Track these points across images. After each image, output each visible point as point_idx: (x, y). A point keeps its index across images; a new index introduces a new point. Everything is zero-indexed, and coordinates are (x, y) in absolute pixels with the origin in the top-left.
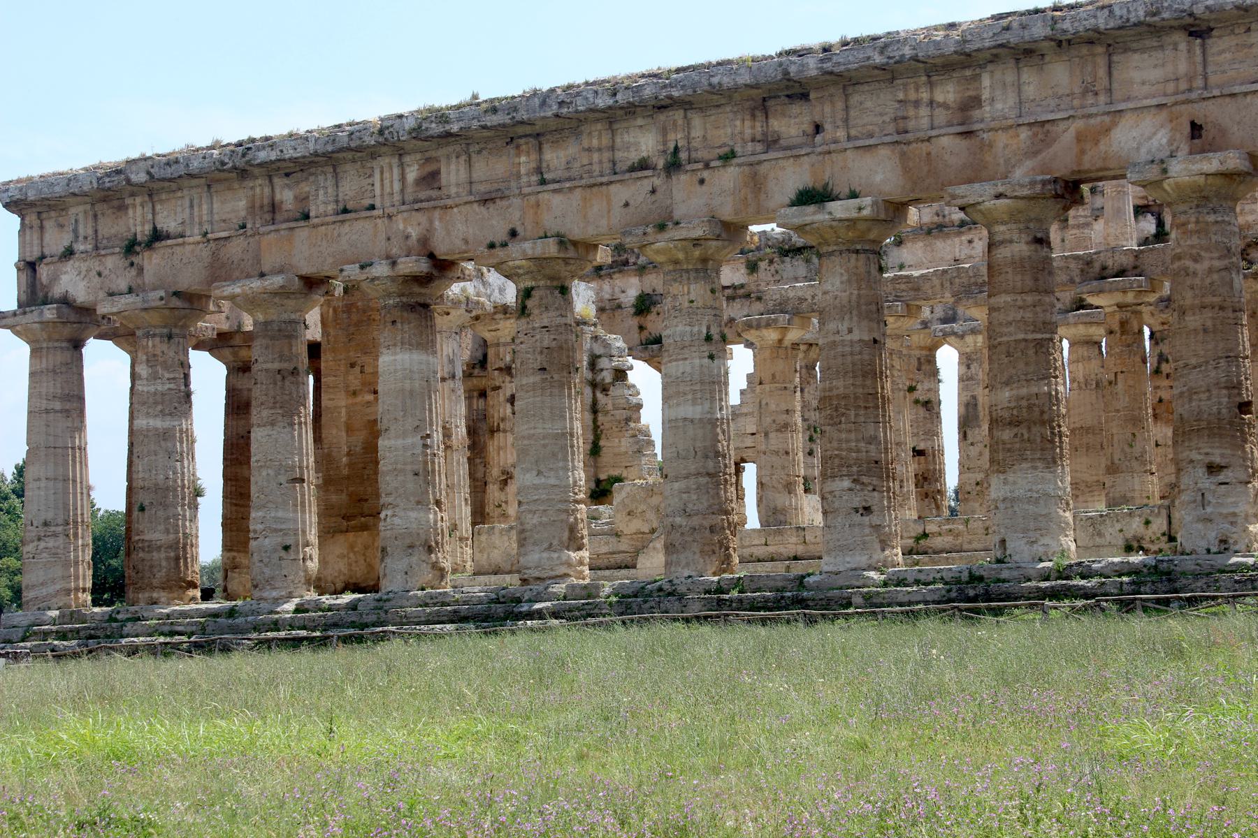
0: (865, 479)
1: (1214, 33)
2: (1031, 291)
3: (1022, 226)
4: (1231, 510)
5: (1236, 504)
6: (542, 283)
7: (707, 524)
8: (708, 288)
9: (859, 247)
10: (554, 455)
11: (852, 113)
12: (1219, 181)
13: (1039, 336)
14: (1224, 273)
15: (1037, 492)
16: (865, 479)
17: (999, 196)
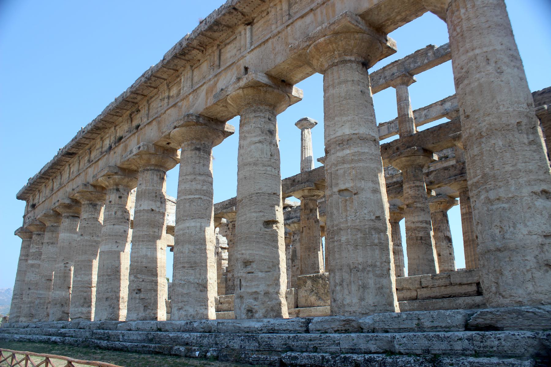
0: (139, 276)
1: (255, 21)
2: (191, 174)
3: (189, 142)
5: (258, 285)
6: (86, 202)
7: (105, 297)
8: (118, 196)
9: (148, 168)
10: (81, 268)
11: (150, 111)
12: (250, 91)
13: (192, 197)
14: (258, 145)
15: (184, 281)
16: (139, 276)
17: (175, 127)
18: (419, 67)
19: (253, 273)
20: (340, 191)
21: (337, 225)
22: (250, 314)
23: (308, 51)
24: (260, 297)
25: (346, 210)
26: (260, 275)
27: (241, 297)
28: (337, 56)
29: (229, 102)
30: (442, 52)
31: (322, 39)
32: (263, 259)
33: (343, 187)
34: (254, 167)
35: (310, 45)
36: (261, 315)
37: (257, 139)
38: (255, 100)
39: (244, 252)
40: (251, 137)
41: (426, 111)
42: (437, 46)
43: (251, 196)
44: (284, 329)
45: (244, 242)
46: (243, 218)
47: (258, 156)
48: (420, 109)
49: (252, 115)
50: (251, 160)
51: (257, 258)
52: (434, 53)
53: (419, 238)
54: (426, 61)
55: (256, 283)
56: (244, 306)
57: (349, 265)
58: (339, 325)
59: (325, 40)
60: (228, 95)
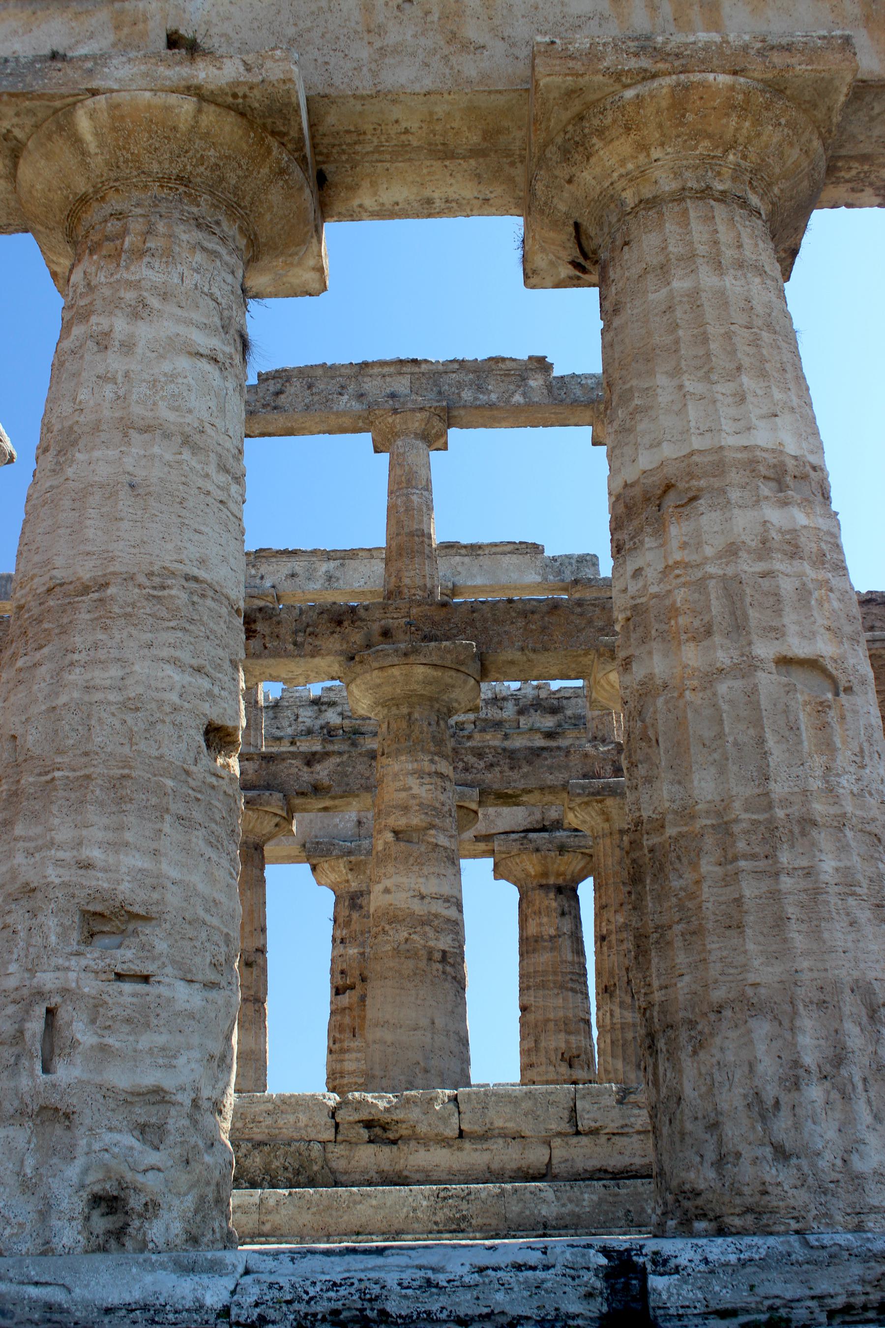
4: (150, 1078)
5: (168, 1056)
12: (226, 128)
14: (206, 366)
18: (491, 406)
19: (145, 979)
20: (785, 662)
21: (786, 803)
22: (100, 1223)
23: (630, 94)
24: (176, 1122)
25: (828, 747)
26: (186, 997)
27: (54, 1115)
28: (727, 172)
29: (84, 124)
30: (578, 392)
31: (724, 79)
32: (201, 913)
33: (800, 649)
34: (186, 455)
35: (654, 76)
36: (177, 1228)
37: (205, 342)
38: (222, 179)
39: (95, 854)
40: (179, 320)
41: (332, 564)
42: (557, 372)
43: (158, 582)
44: (462, 1311)
45: (102, 804)
46: (99, 676)
47: (205, 416)
48: (314, 552)
49: (187, 235)
50: (172, 416)
51: (173, 899)
52: (549, 387)
53: (437, 956)
54: (518, 398)
55: (161, 1039)
56: (73, 1172)
57: (863, 989)
58: (863, 1281)
59: (732, 88)
60: (94, 93)
